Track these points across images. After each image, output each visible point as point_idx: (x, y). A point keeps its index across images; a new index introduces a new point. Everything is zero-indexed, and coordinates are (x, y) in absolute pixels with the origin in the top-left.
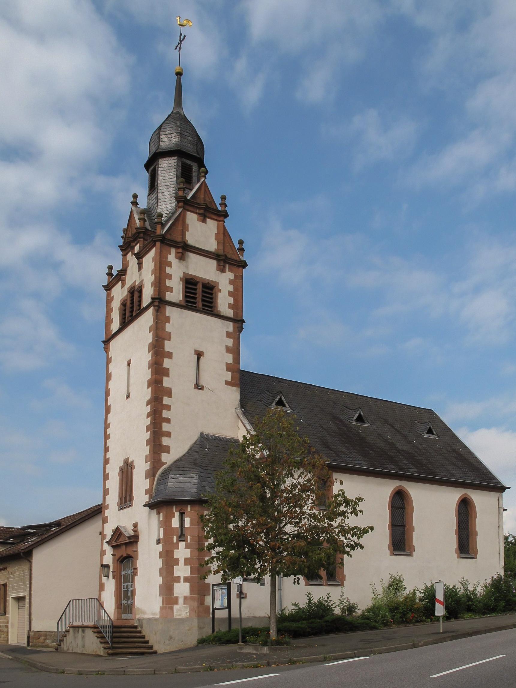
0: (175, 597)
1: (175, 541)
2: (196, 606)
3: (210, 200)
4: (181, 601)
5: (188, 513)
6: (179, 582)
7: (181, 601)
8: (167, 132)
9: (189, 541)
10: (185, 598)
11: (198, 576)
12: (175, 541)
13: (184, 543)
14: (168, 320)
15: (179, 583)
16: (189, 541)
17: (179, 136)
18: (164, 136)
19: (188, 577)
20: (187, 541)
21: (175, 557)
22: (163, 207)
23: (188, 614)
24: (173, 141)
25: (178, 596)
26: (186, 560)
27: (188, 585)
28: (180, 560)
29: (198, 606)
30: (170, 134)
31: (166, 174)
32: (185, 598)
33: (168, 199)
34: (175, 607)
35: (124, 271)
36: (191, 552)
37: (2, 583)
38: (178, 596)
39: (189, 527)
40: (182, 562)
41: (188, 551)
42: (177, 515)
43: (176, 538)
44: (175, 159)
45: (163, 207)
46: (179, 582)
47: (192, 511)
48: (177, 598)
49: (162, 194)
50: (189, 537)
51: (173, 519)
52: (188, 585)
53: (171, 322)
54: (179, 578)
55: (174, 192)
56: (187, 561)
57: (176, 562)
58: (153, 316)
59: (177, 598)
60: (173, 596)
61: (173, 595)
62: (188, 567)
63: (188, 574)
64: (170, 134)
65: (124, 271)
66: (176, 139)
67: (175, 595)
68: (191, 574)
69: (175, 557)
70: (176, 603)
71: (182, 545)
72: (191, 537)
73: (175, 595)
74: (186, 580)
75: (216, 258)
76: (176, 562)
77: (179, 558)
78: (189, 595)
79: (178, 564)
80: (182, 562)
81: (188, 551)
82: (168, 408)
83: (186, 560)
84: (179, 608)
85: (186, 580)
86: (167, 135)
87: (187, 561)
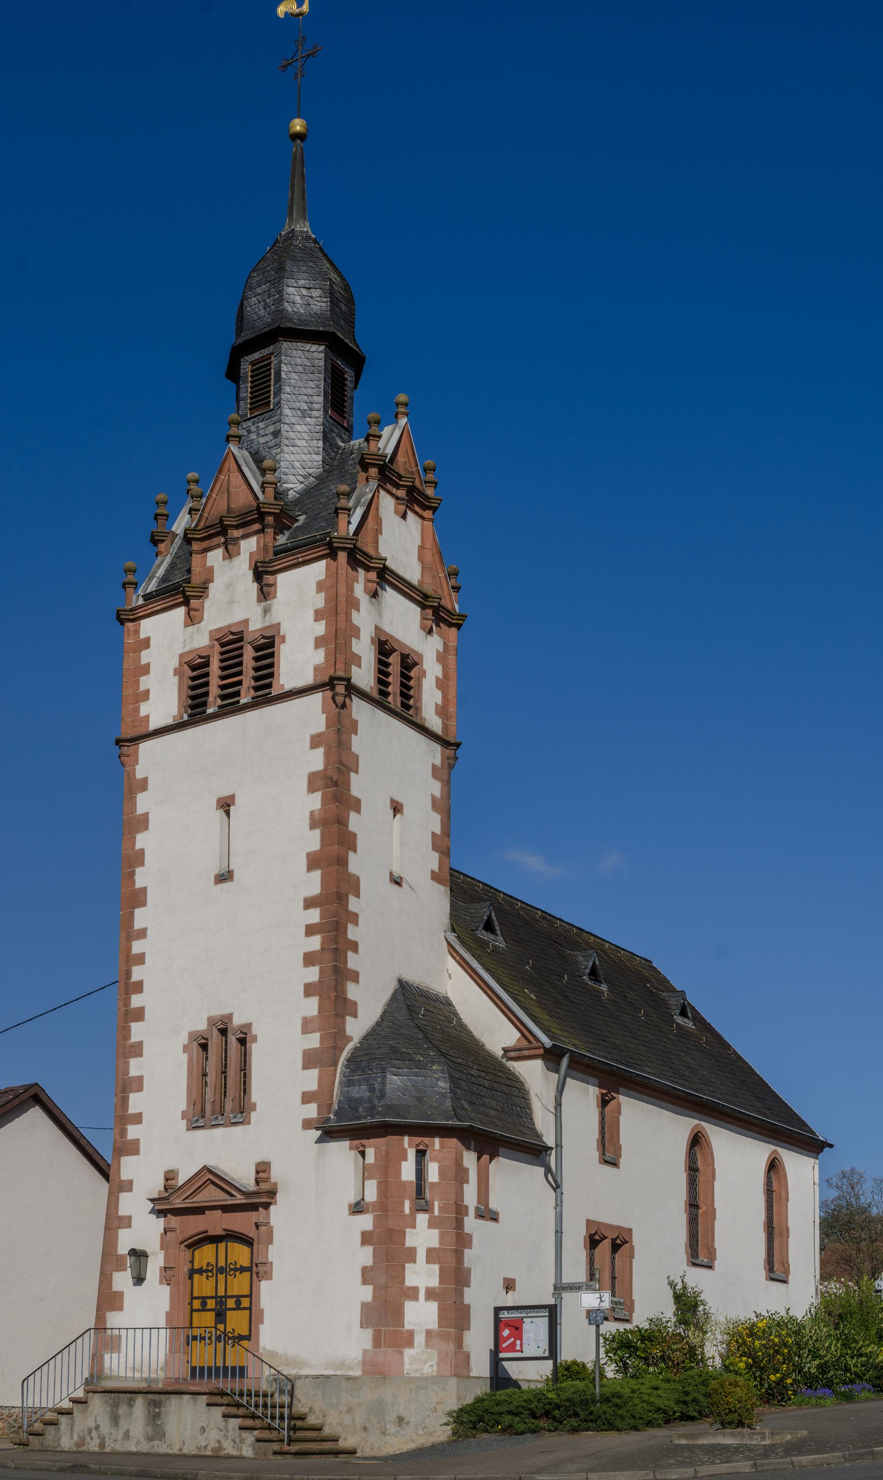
0: (408, 1331)
1: (407, 1211)
2: (452, 1352)
3: (411, 468)
4: (420, 1339)
5: (436, 1152)
6: (416, 1299)
7: (420, 1339)
8: (302, 282)
9: (436, 1213)
10: (429, 1333)
11: (455, 1288)
12: (407, 1211)
13: (427, 1215)
14: (354, 727)
15: (416, 1301)
16: (436, 1213)
17: (329, 299)
18: (293, 289)
19: (435, 1288)
20: (433, 1212)
21: (408, 1244)
22: (292, 457)
23: (435, 1368)
24: (314, 306)
25: (414, 1330)
26: (430, 1251)
27: (434, 1306)
28: (418, 1250)
29: (455, 1352)
30: (309, 289)
31: (299, 382)
32: (429, 1333)
33: (304, 443)
34: (408, 1353)
35: (201, 590)
36: (442, 1236)
37: (428, 1151)
38: (414, 1330)
39: (436, 1183)
40: (421, 1255)
41: (435, 1233)
42: (411, 1154)
43: (410, 1204)
44: (320, 350)
45: (292, 457)
46: (416, 1299)
47: (443, 1148)
48: (411, 1334)
49: (291, 428)
50: (436, 1204)
51: (404, 1164)
52: (434, 1306)
53: (359, 732)
54: (415, 1290)
55: (318, 427)
56: (432, 1255)
57: (411, 1255)
58: (323, 713)
59: (411, 1334)
60: (402, 1329)
61: (404, 1327)
62: (436, 1268)
63: (434, 1282)
64: (309, 289)
65: (201, 590)
66: (322, 304)
67: (407, 1326)
68: (440, 1283)
69: (408, 1244)
70: (410, 1344)
71: (422, 1219)
72: (442, 1205)
73: (407, 1326)
74: (431, 1294)
75: (422, 601)
76: (411, 1255)
77: (415, 1248)
78: (436, 1327)
79: (414, 1261)
80: (421, 1255)
81: (435, 1233)
82: (310, 930)
83: (430, 1251)
84: (414, 1354)
85: (431, 1294)
86: (301, 289)
87: (432, 1255)
